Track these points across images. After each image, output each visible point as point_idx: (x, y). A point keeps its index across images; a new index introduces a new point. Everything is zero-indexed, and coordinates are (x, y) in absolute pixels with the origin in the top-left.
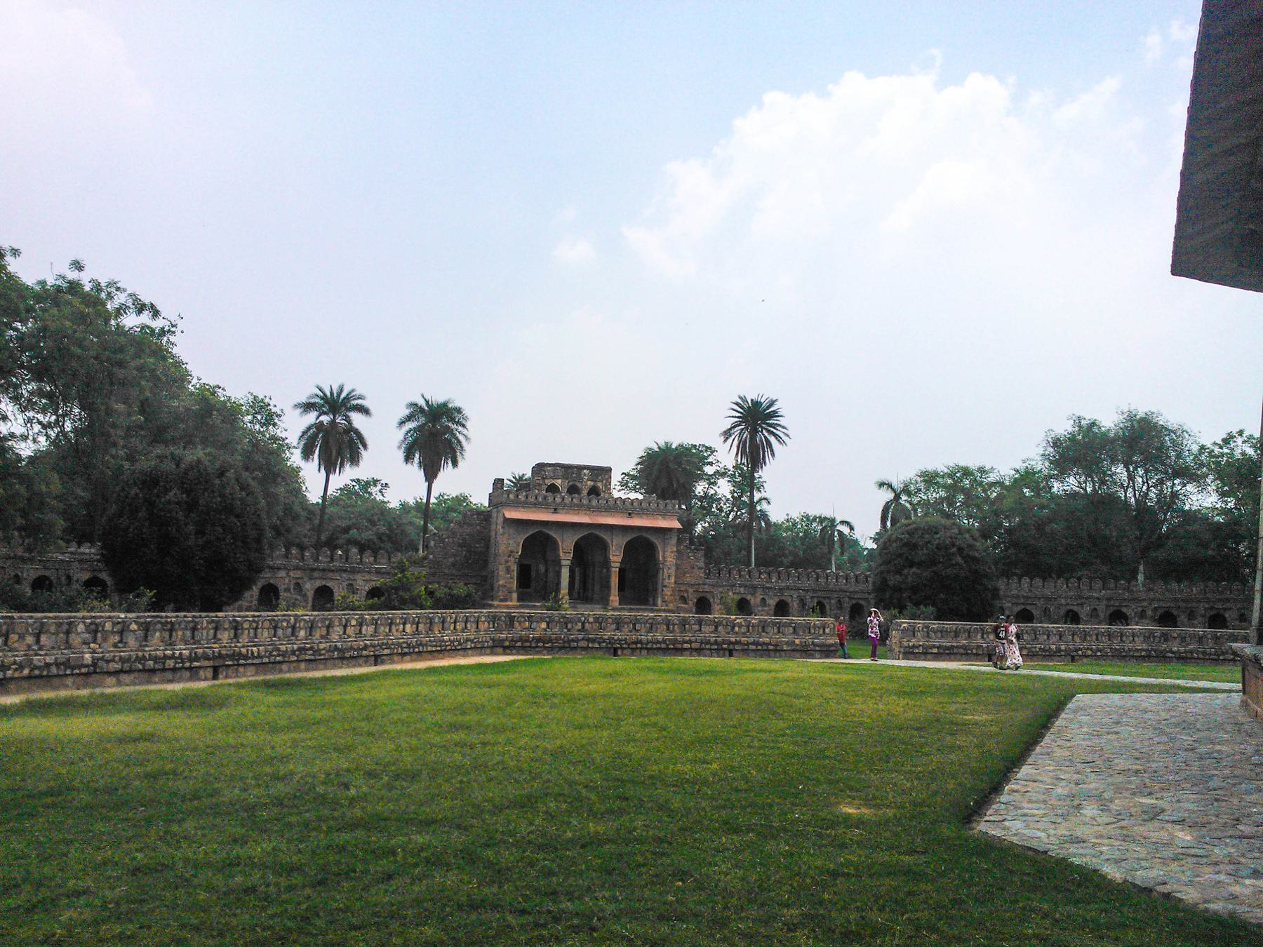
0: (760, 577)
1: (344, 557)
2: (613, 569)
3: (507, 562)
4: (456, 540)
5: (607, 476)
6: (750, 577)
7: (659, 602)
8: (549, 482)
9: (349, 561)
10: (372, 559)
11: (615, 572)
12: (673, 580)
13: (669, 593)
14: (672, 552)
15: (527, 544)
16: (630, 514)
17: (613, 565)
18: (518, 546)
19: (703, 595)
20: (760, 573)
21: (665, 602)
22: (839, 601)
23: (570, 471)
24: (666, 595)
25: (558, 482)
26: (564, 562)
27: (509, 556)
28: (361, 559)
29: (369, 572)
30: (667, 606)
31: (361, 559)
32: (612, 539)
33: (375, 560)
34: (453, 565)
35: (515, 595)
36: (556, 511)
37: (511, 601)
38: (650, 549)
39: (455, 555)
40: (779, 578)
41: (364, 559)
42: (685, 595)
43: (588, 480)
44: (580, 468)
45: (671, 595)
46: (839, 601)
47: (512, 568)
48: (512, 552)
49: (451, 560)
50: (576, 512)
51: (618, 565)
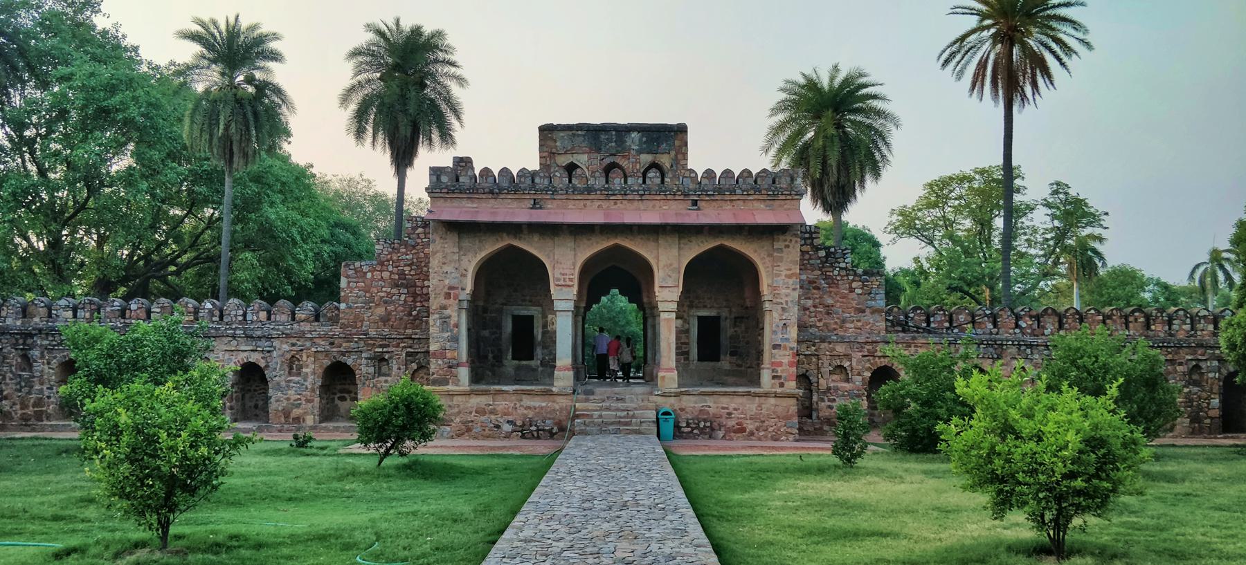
0: (1017, 326)
1: (217, 313)
2: (663, 316)
3: (444, 307)
4: (386, 275)
5: (677, 143)
6: (995, 325)
7: (766, 376)
8: (564, 160)
9: (225, 320)
10: (263, 315)
11: (668, 320)
12: (793, 332)
13: (785, 360)
14: (789, 277)
15: (486, 272)
16: (695, 203)
17: (661, 306)
18: (464, 276)
19: (884, 362)
20: (1018, 318)
21: (774, 377)
22: (1197, 367)
23: (603, 137)
24: (780, 364)
25: (582, 159)
26: (558, 305)
27: (448, 296)
28: (245, 315)
29: (234, 337)
30: (782, 385)
31: (245, 315)
32: (657, 258)
33: (269, 318)
34: (385, 320)
35: (464, 373)
36: (536, 205)
37: (457, 383)
38: (746, 274)
39: (386, 302)
40: (1061, 327)
41: (249, 317)
42: (846, 364)
43: (640, 152)
44: (622, 131)
45: (791, 364)
46: (1197, 367)
47: (454, 320)
48: (451, 288)
49: (380, 311)
50: (582, 203)
51: (674, 306)
